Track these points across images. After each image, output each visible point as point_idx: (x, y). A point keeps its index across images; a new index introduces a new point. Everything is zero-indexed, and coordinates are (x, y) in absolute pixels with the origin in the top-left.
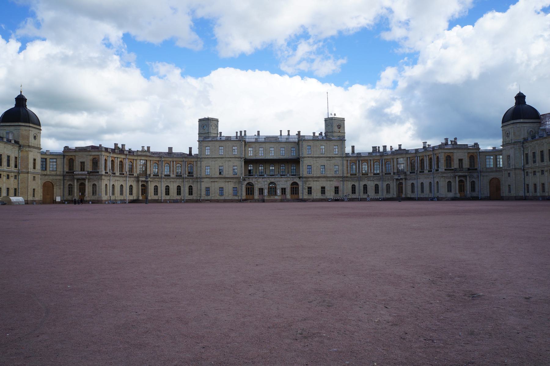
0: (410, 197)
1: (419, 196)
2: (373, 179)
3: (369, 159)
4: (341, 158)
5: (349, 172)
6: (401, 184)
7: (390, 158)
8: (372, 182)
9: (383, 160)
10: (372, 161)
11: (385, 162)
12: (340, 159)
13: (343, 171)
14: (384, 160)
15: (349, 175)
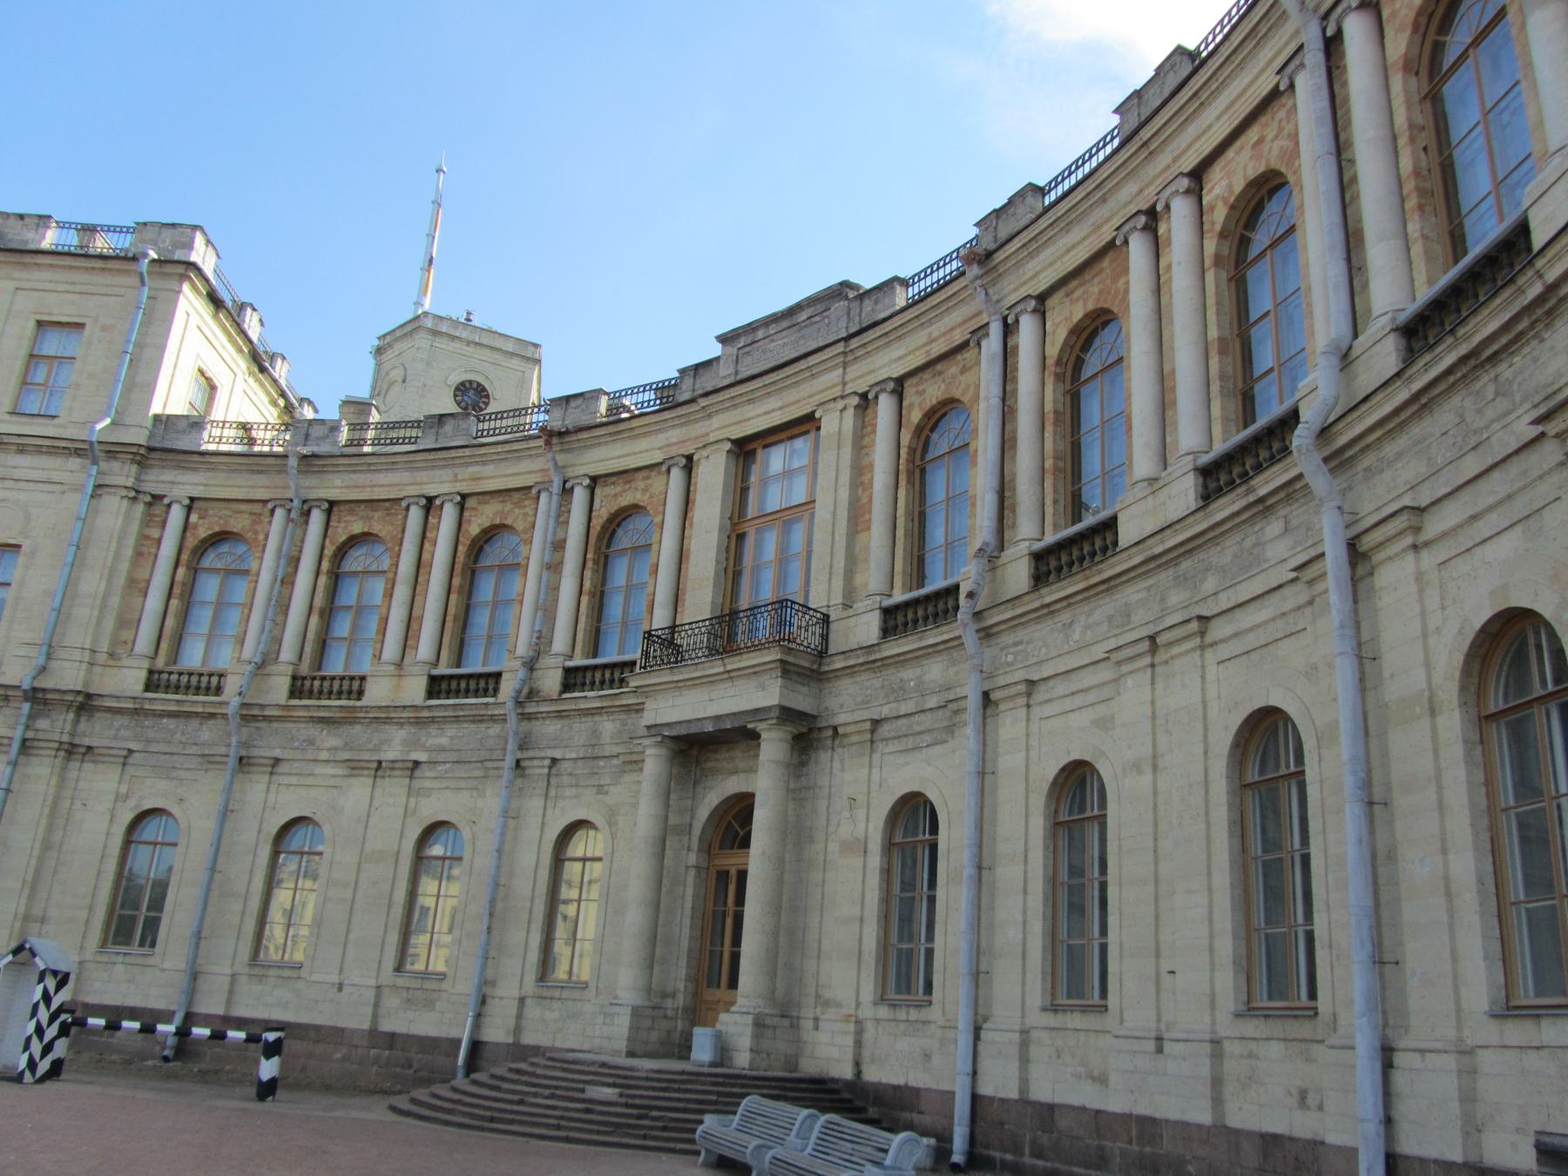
0: (845, 1072)
1: (999, 1082)
2: (414, 744)
3: (413, 490)
4: (74, 463)
5: (144, 641)
6: (737, 815)
7: (658, 457)
8: (394, 790)
9: (567, 492)
10: (449, 513)
11: (602, 512)
12: (70, 470)
13: (61, 615)
14: (580, 495)
15: (129, 680)
